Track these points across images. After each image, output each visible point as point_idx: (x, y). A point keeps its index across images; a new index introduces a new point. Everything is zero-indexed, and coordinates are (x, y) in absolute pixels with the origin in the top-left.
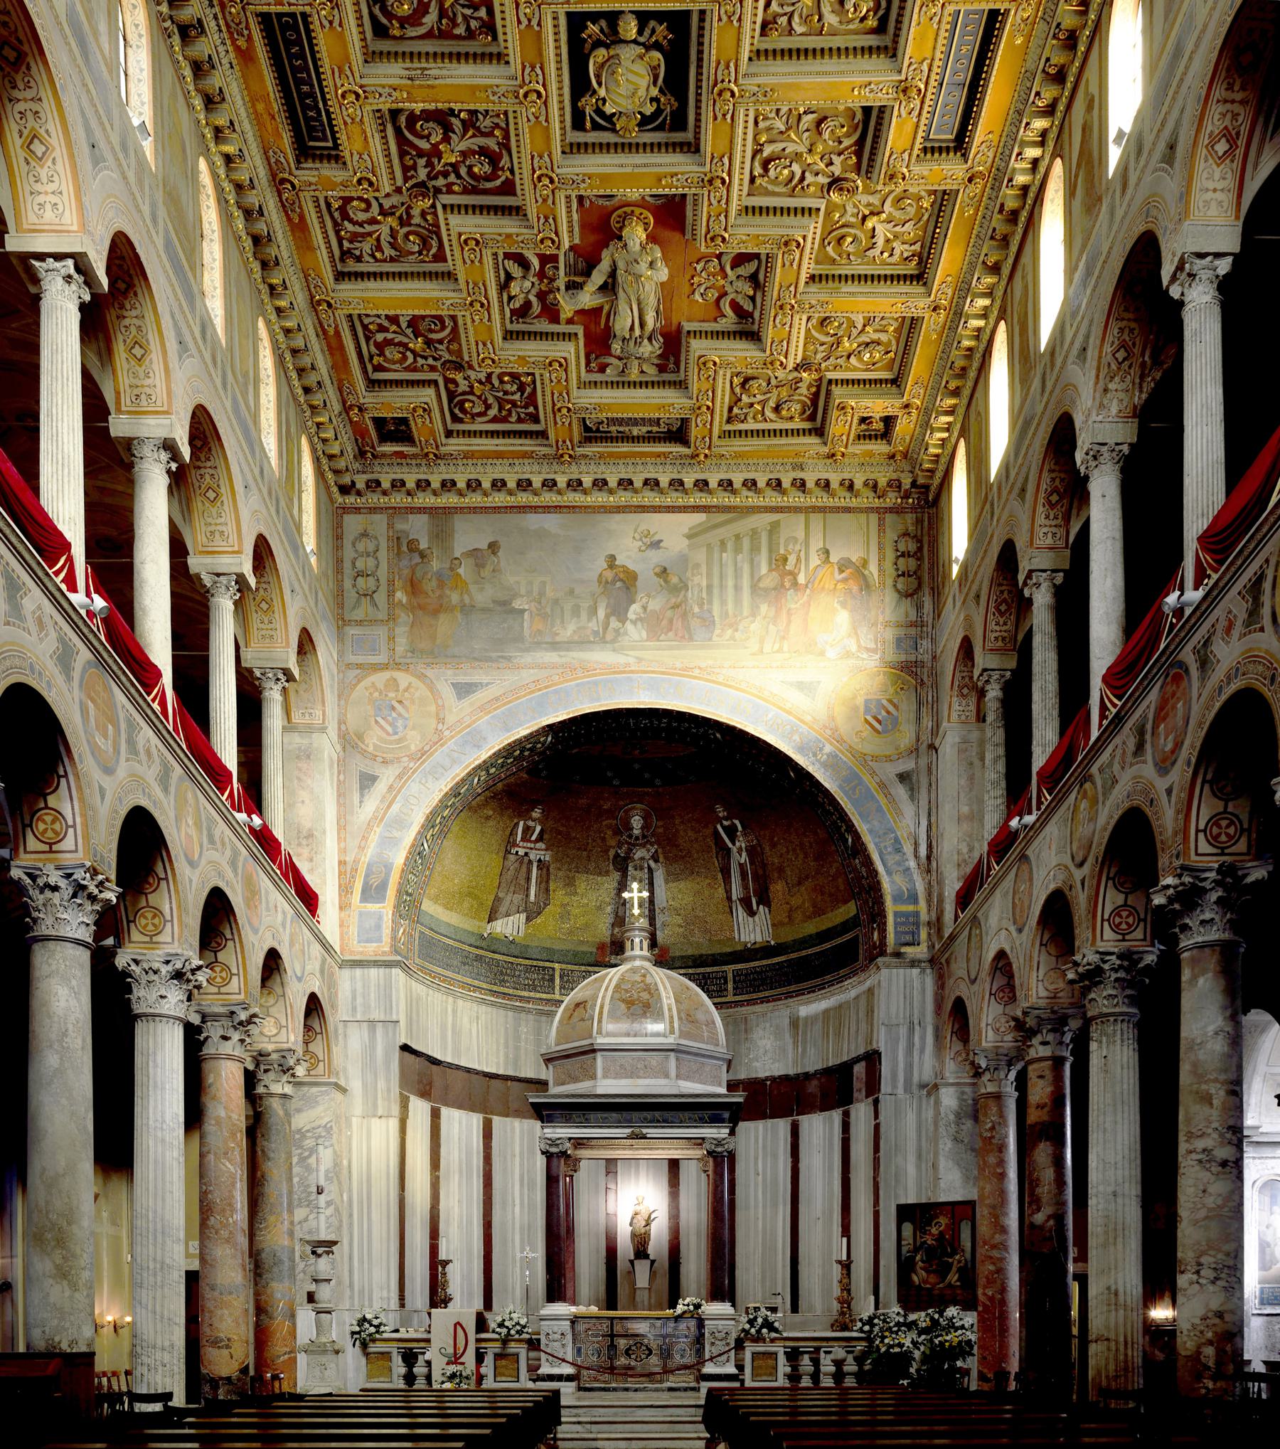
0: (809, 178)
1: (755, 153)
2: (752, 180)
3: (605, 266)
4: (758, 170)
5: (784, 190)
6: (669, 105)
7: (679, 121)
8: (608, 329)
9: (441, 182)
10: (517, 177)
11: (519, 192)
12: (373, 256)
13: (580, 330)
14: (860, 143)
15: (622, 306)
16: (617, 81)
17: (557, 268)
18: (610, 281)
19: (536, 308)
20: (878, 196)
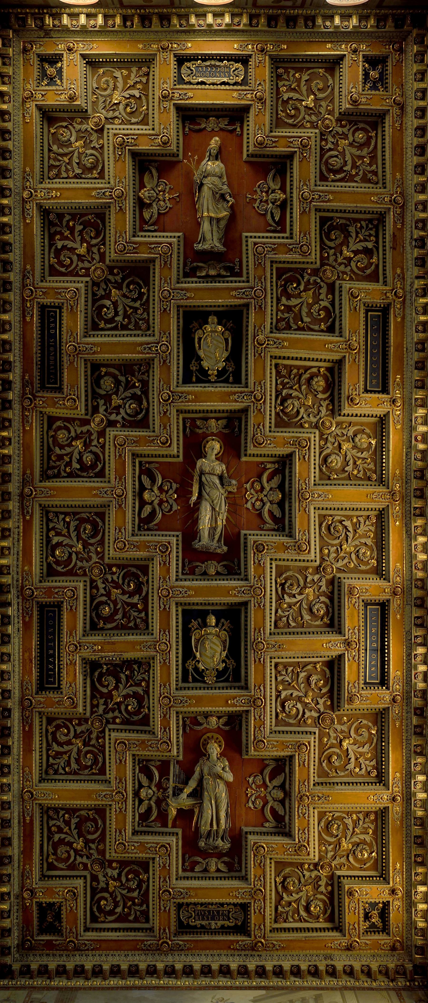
0: (308, 714)
1: (278, 696)
2: (277, 715)
3: (196, 775)
4: (279, 709)
5: (294, 722)
6: (232, 663)
7: (236, 676)
8: (197, 828)
9: (110, 715)
10: (151, 712)
11: (151, 723)
12: (64, 769)
13: (180, 831)
14: (331, 691)
15: (206, 804)
16: (205, 647)
17: (168, 779)
18: (199, 788)
19: (155, 814)
20: (346, 725)
